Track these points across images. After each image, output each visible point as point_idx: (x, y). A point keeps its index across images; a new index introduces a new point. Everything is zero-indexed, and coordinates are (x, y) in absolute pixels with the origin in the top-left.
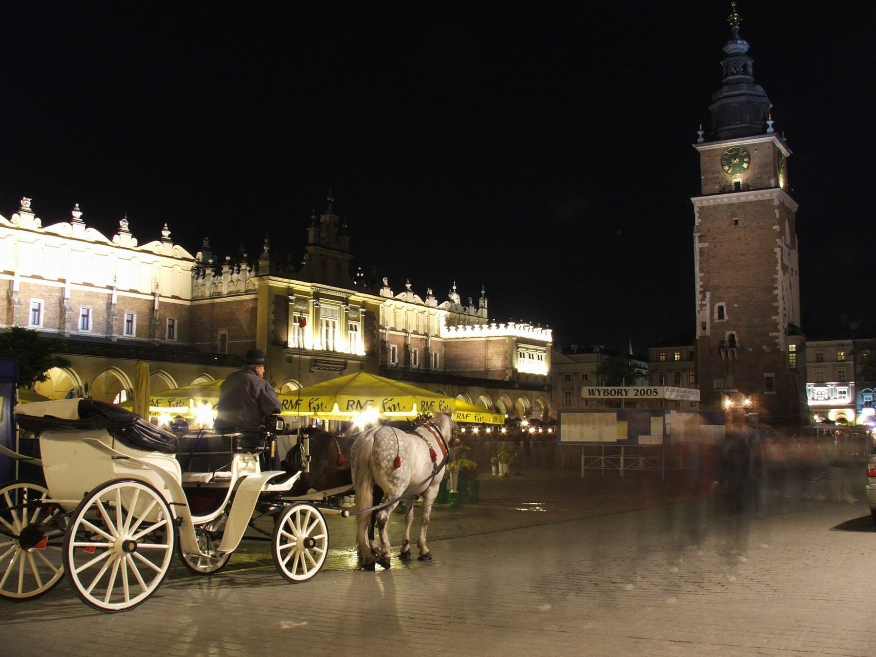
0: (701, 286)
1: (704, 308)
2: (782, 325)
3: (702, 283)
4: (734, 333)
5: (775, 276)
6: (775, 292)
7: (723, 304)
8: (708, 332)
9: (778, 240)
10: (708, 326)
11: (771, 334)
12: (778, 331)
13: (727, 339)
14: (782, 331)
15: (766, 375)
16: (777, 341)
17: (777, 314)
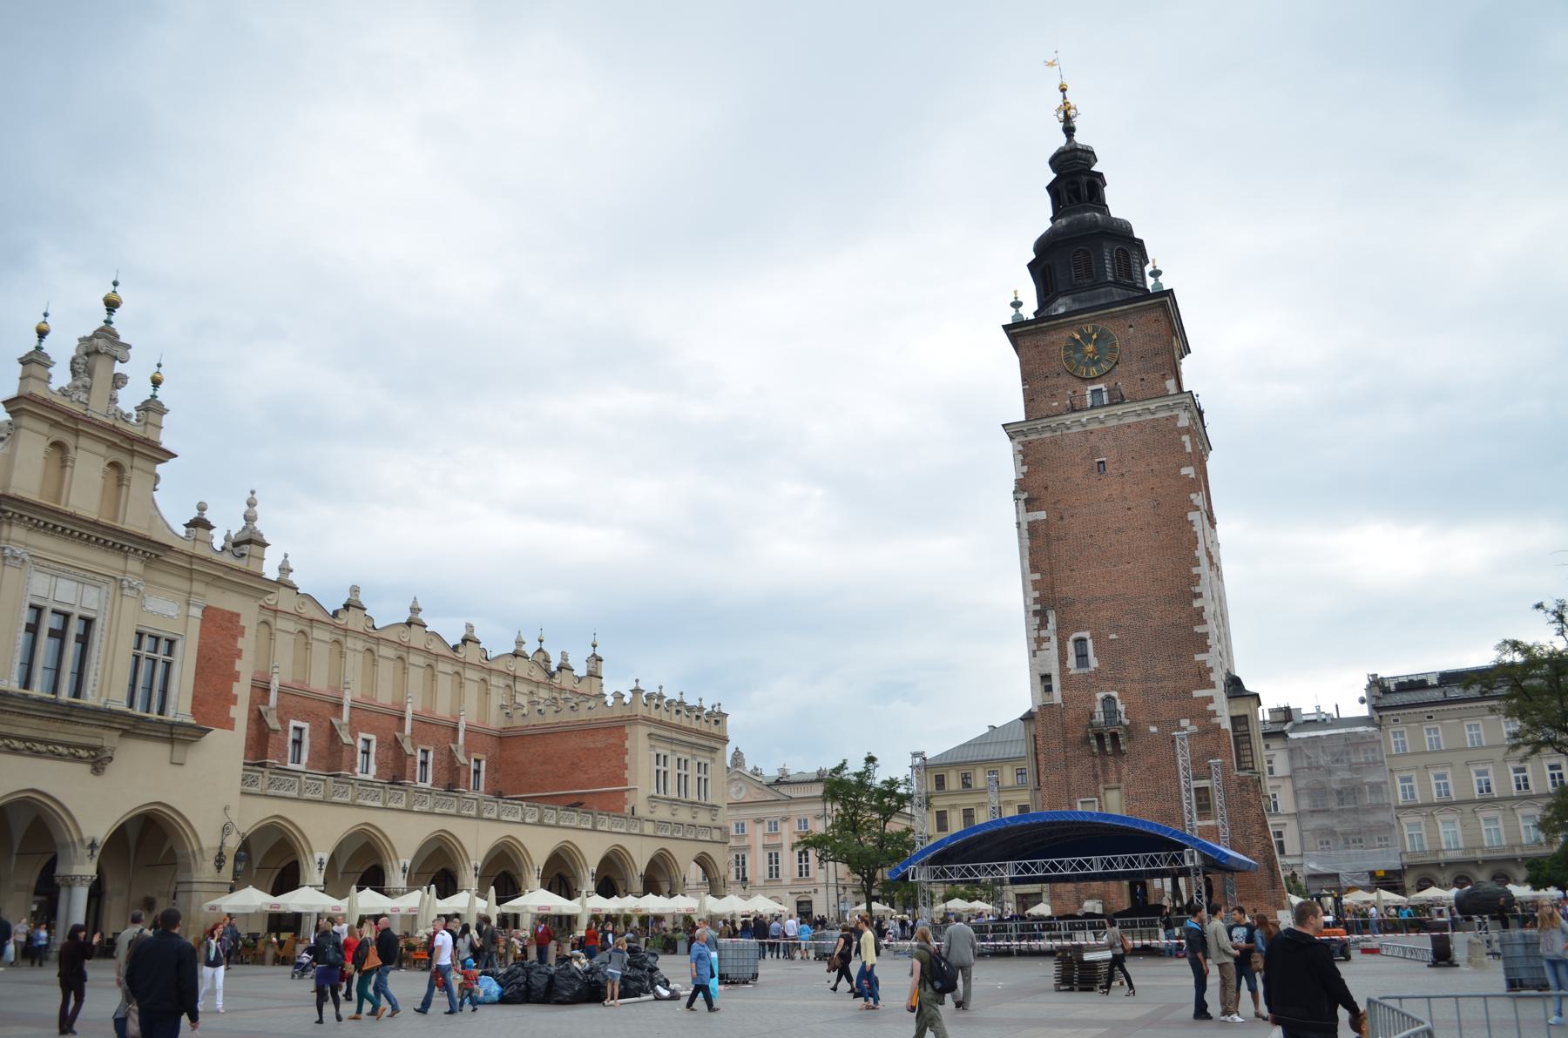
0: (1036, 601)
1: (1045, 645)
2: (1218, 677)
3: (1037, 594)
4: (1115, 694)
5: (1195, 570)
6: (1197, 604)
7: (1086, 635)
8: (1057, 697)
9: (1193, 496)
10: (1056, 683)
11: (1197, 694)
12: (1212, 685)
13: (1099, 708)
14: (1220, 686)
15: (1195, 784)
16: (1211, 707)
17: (1205, 649)
